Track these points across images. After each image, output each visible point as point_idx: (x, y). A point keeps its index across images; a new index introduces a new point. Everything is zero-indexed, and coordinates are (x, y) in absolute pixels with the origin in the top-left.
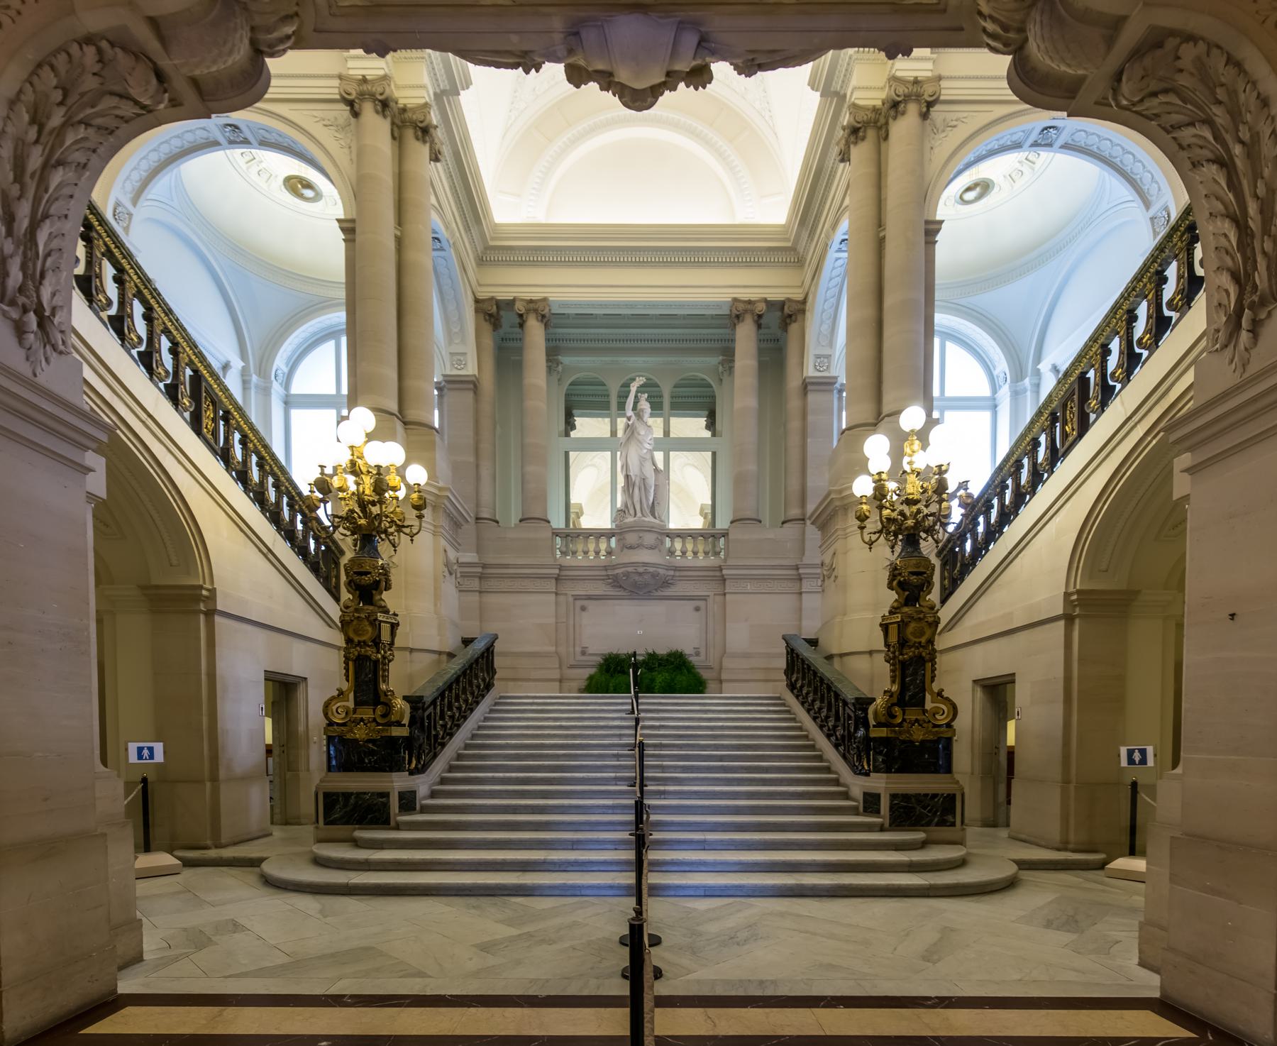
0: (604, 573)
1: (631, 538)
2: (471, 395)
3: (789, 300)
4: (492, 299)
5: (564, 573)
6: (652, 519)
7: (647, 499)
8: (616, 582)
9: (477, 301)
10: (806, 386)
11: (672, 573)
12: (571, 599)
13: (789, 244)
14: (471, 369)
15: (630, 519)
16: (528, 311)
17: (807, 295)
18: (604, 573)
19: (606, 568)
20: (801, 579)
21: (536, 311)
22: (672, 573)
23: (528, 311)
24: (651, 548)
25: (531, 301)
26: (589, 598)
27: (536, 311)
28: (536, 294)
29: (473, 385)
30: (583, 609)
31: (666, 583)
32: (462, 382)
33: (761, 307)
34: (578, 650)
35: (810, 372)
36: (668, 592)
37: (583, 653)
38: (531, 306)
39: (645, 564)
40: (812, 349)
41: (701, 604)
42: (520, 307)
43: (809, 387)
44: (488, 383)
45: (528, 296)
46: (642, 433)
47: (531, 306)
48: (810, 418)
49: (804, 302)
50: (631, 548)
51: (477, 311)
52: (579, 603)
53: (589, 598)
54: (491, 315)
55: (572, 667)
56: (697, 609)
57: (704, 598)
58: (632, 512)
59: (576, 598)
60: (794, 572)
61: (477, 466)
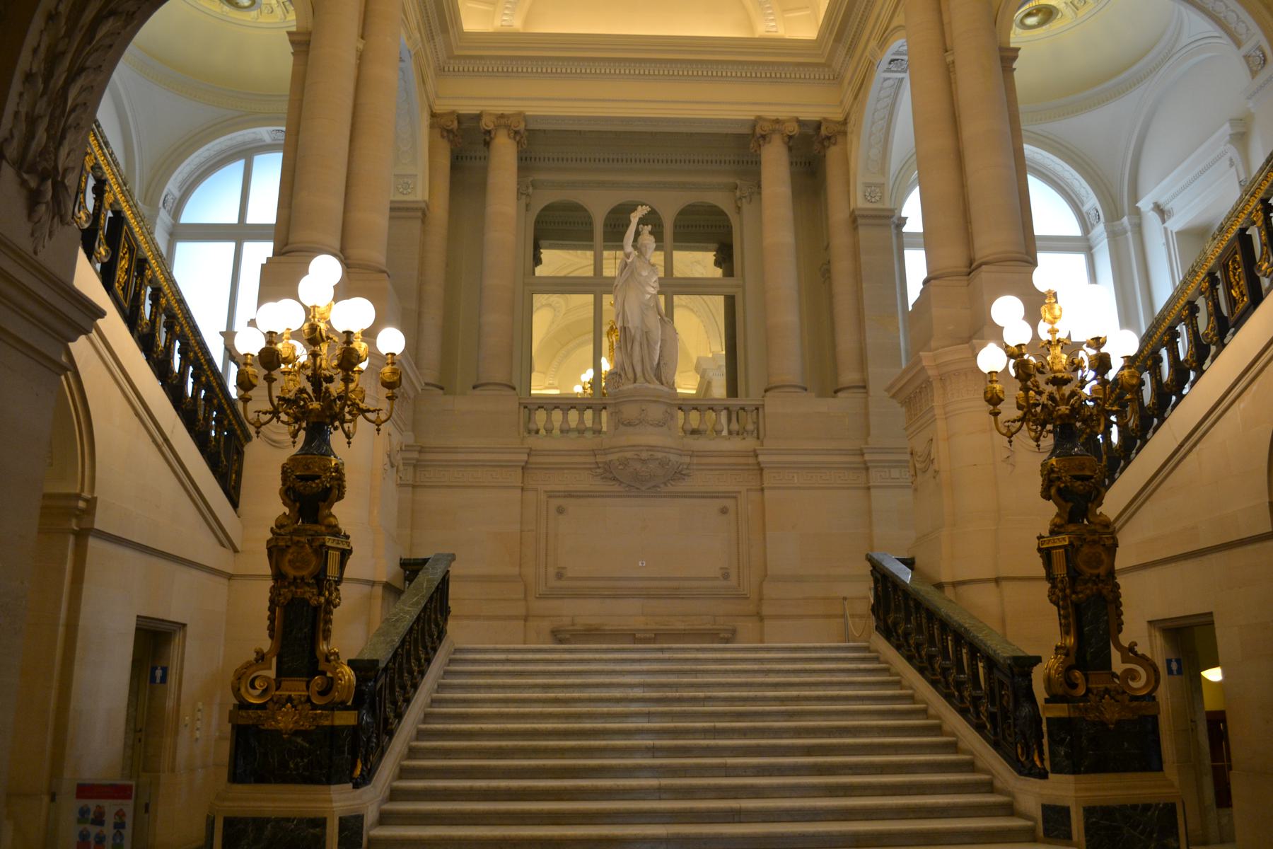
0: (591, 459)
1: (630, 411)
2: (417, 224)
3: (825, 119)
4: (453, 113)
5: (532, 459)
6: (659, 387)
7: (651, 359)
8: (608, 472)
9: (433, 115)
10: (854, 220)
11: (687, 459)
12: (543, 497)
13: (823, 61)
14: (419, 193)
15: (629, 386)
16: (497, 127)
17: (848, 115)
18: (591, 459)
19: (594, 453)
20: (867, 469)
21: (508, 127)
22: (687, 459)
23: (497, 127)
24: (660, 425)
25: (502, 116)
26: (570, 495)
27: (508, 127)
28: (509, 107)
29: (423, 213)
30: (560, 510)
31: (679, 474)
32: (407, 209)
33: (793, 129)
34: (552, 571)
35: (859, 202)
36: (681, 486)
37: (559, 576)
38: (502, 121)
39: (651, 448)
40: (861, 176)
41: (729, 503)
42: (487, 123)
43: (860, 221)
44: (440, 212)
45: (500, 110)
46: (645, 273)
47: (502, 121)
48: (863, 258)
49: (845, 122)
50: (630, 424)
51: (432, 126)
52: (555, 502)
53: (570, 495)
54: (449, 131)
55: (542, 597)
56: (724, 511)
57: (733, 496)
58: (631, 375)
59: (551, 495)
60: (858, 459)
61: (420, 315)
